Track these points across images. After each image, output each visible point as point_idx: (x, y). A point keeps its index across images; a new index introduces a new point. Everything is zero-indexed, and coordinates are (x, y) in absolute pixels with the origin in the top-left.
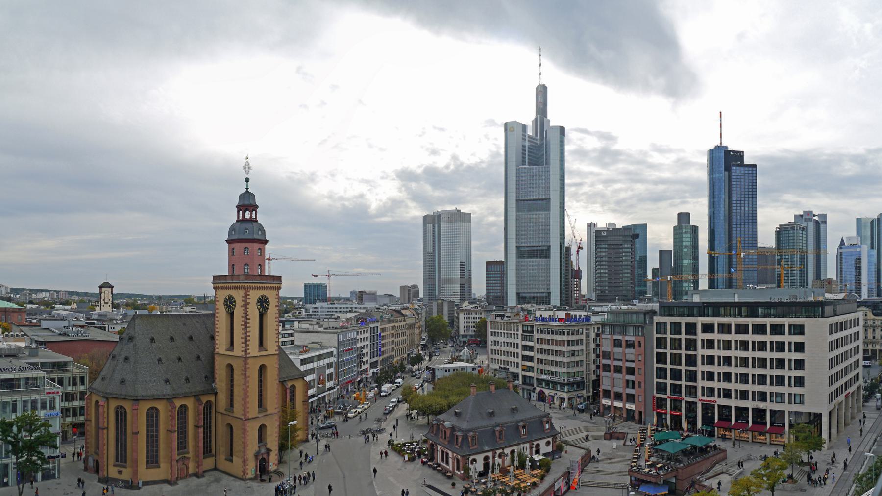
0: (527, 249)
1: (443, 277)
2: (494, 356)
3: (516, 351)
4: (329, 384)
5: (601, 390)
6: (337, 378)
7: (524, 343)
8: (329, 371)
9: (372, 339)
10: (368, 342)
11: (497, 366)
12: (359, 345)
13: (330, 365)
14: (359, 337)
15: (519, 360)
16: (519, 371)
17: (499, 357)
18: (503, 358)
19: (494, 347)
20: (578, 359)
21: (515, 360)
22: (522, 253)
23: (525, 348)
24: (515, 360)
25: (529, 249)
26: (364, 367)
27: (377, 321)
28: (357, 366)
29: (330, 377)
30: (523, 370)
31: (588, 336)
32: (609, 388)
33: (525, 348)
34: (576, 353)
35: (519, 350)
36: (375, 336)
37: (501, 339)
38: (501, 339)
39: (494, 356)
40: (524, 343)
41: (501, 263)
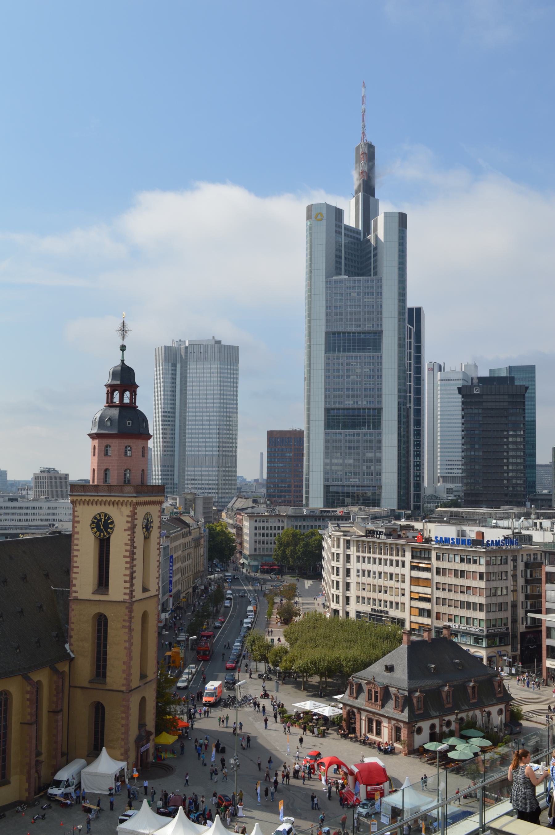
5: (544, 647)
15: (406, 599)
19: (362, 580)
20: (500, 600)
23: (415, 581)
24: (400, 599)
33: (415, 581)
37: (376, 568)
38: (376, 568)
40: (415, 574)
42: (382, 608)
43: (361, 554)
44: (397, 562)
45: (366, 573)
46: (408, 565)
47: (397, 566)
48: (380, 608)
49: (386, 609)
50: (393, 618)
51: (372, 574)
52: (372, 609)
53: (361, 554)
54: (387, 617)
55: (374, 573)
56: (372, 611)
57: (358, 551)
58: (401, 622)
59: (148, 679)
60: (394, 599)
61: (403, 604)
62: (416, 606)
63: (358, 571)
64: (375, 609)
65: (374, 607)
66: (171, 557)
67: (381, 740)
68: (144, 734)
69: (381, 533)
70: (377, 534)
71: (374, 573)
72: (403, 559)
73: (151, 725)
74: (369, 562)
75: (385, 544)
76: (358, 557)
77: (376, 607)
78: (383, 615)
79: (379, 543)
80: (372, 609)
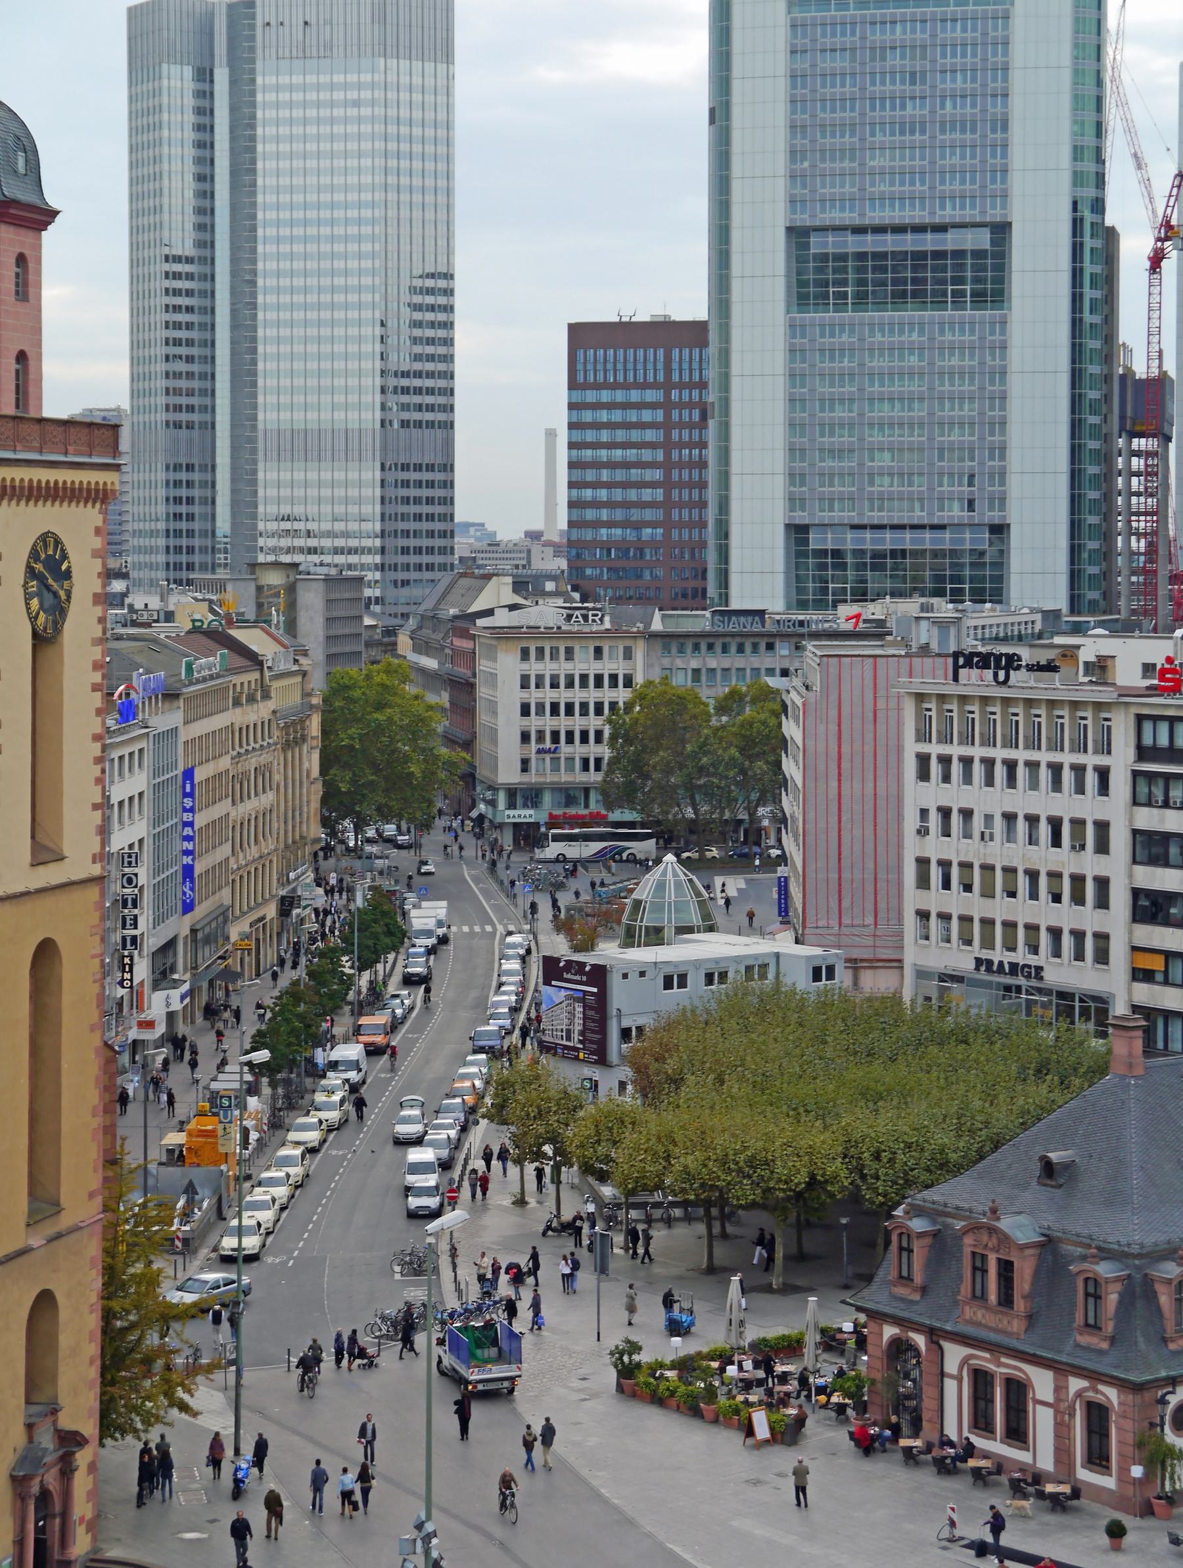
0: (852, 244)
1: (267, 418)
2: (935, 899)
3: (1090, 864)
7: (1149, 819)
11: (962, 960)
15: (1117, 920)
16: (1115, 984)
17: (977, 906)
18: (1000, 909)
19: (935, 847)
21: (1088, 919)
22: (840, 272)
24: (1088, 919)
25: (870, 243)
30: (1142, 975)
35: (1119, 868)
39: (935, 899)
41: (694, 333)
42: (1021, 956)
43: (934, 749)
44: (1079, 770)
45: (956, 820)
46: (1120, 783)
47: (1080, 789)
48: (1008, 957)
49: (1032, 960)
50: (1062, 995)
51: (978, 823)
52: (979, 962)
53: (934, 749)
54: (1040, 991)
55: (989, 818)
56: (977, 969)
57: (923, 736)
58: (1096, 1008)
59: (66, 1221)
60: (1066, 916)
61: (1102, 938)
62: (1156, 944)
63: (924, 813)
64: (990, 963)
65: (985, 954)
66: (189, 774)
67: (1023, 1456)
68: (46, 1440)
69: (1012, 662)
70: (998, 667)
71: (989, 818)
72: (1102, 760)
73: (79, 1409)
74: (968, 779)
75: (1029, 703)
76: (923, 760)
77: (998, 955)
78: (1021, 981)
79: (1007, 702)
80: (979, 962)
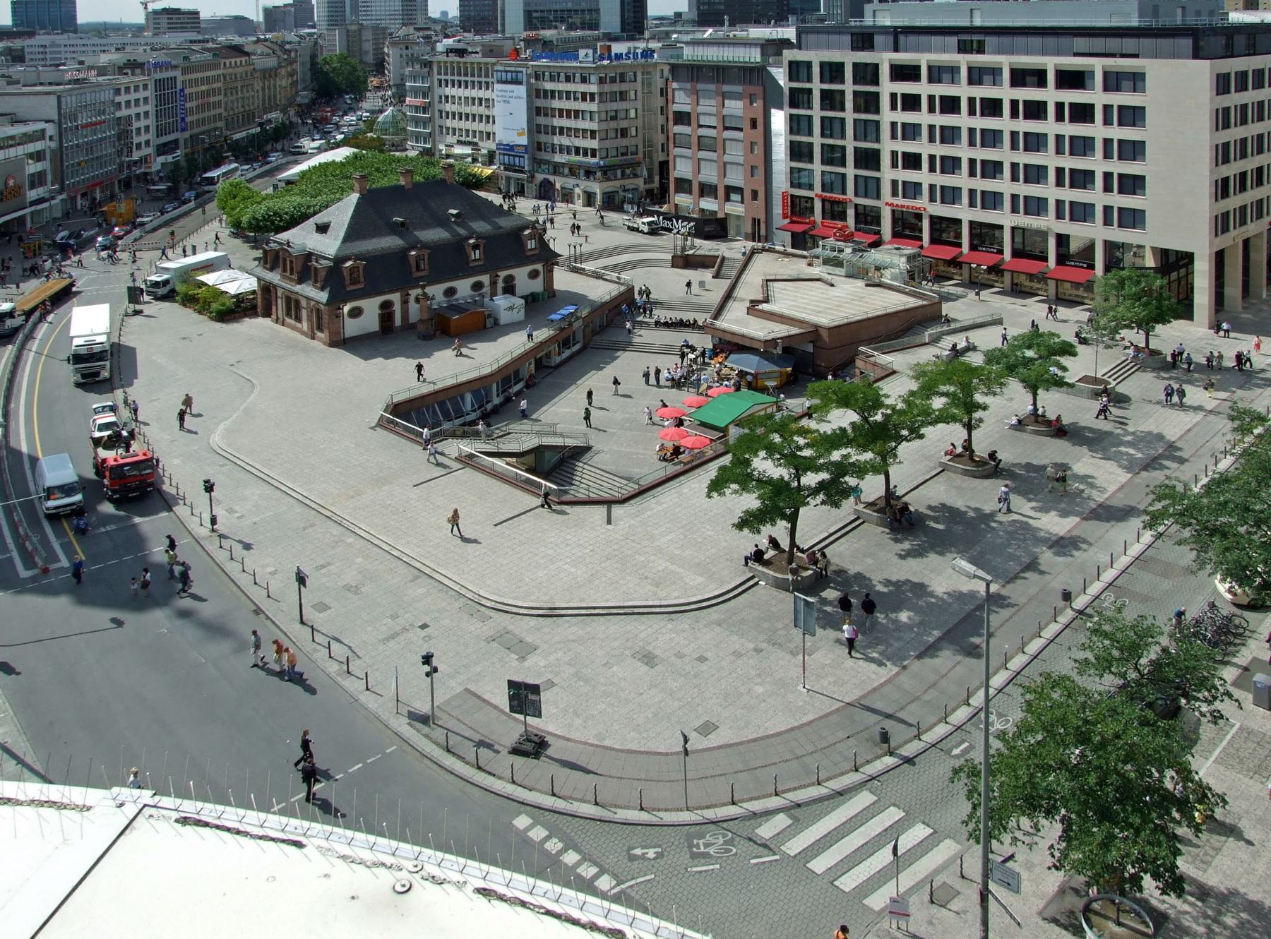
4: (33, 195)
6: (60, 177)
8: (33, 168)
9: (160, 100)
10: (150, 108)
12: (124, 112)
13: (38, 156)
14: (122, 98)
26: (136, 155)
27: (175, 67)
28: (120, 153)
29: (37, 180)
31: (648, 84)
32: (689, 176)
34: (622, 115)
36: (166, 94)
43: (443, 77)
53: (443, 77)
57: (439, 74)
76: (440, 81)
